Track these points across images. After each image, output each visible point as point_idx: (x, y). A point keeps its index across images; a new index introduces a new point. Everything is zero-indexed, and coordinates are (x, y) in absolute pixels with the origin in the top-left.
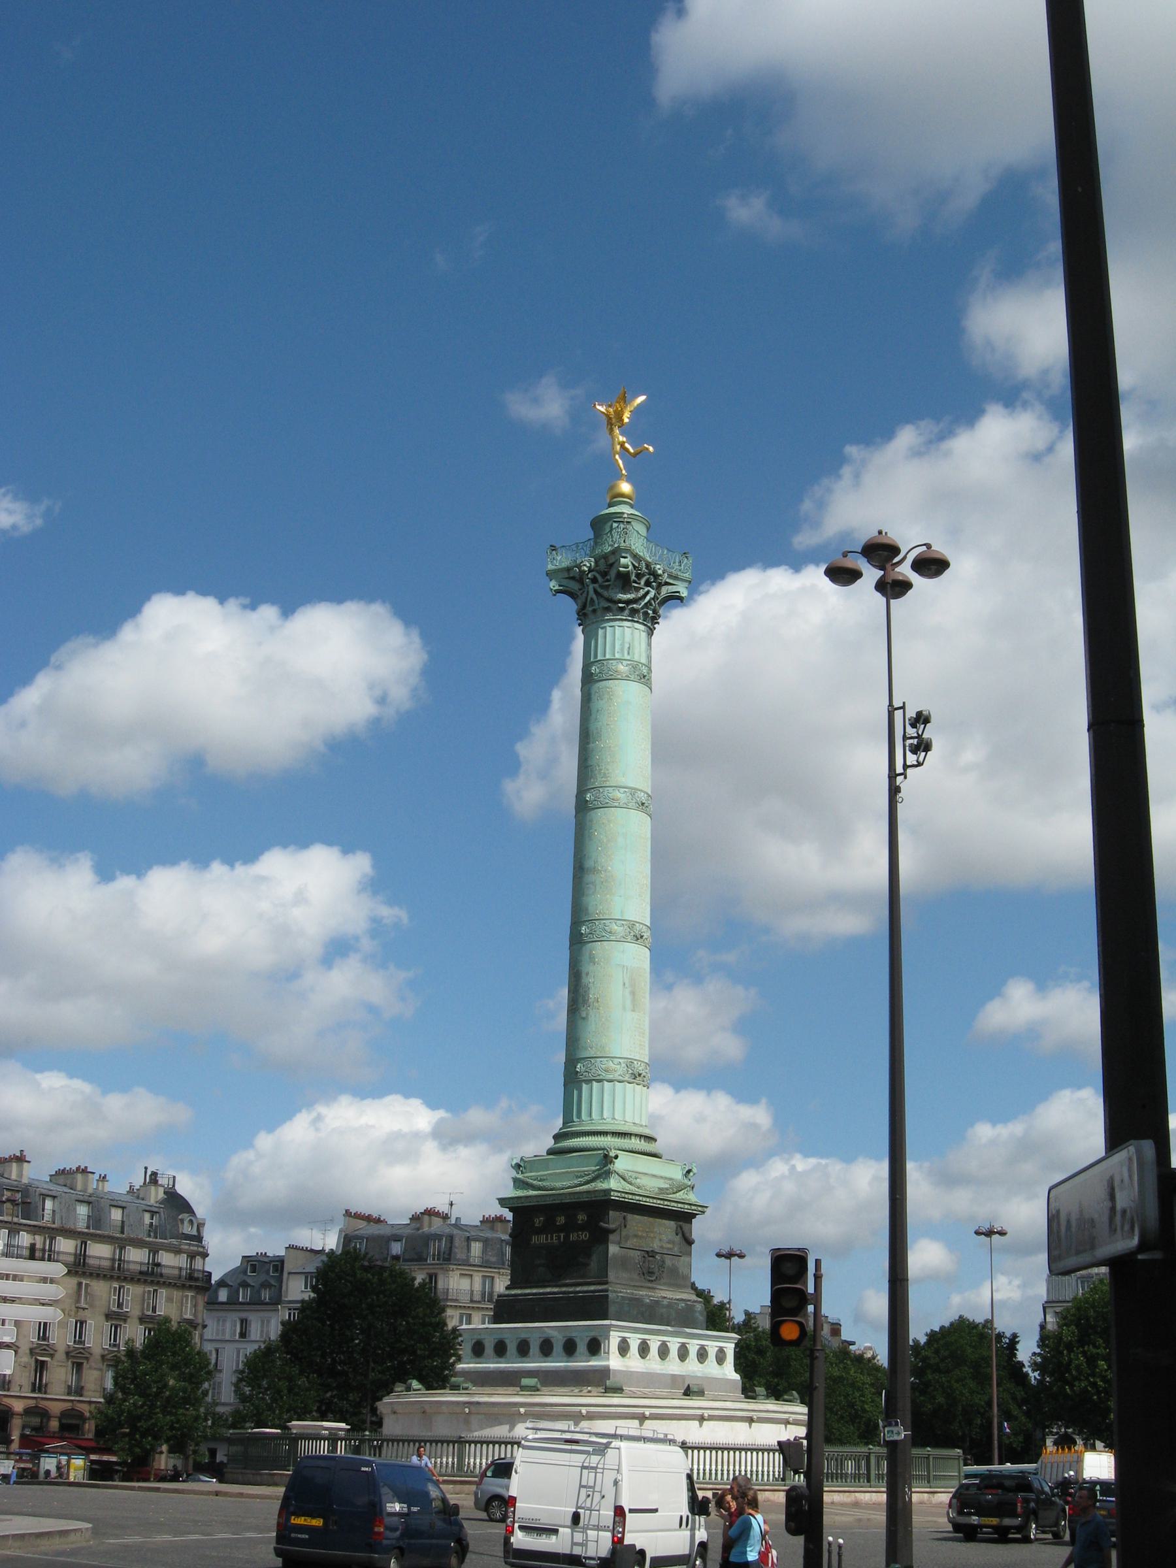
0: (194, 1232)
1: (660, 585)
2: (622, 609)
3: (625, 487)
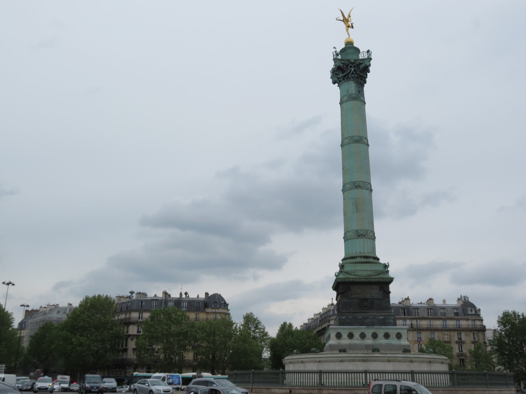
0: (473, 312)
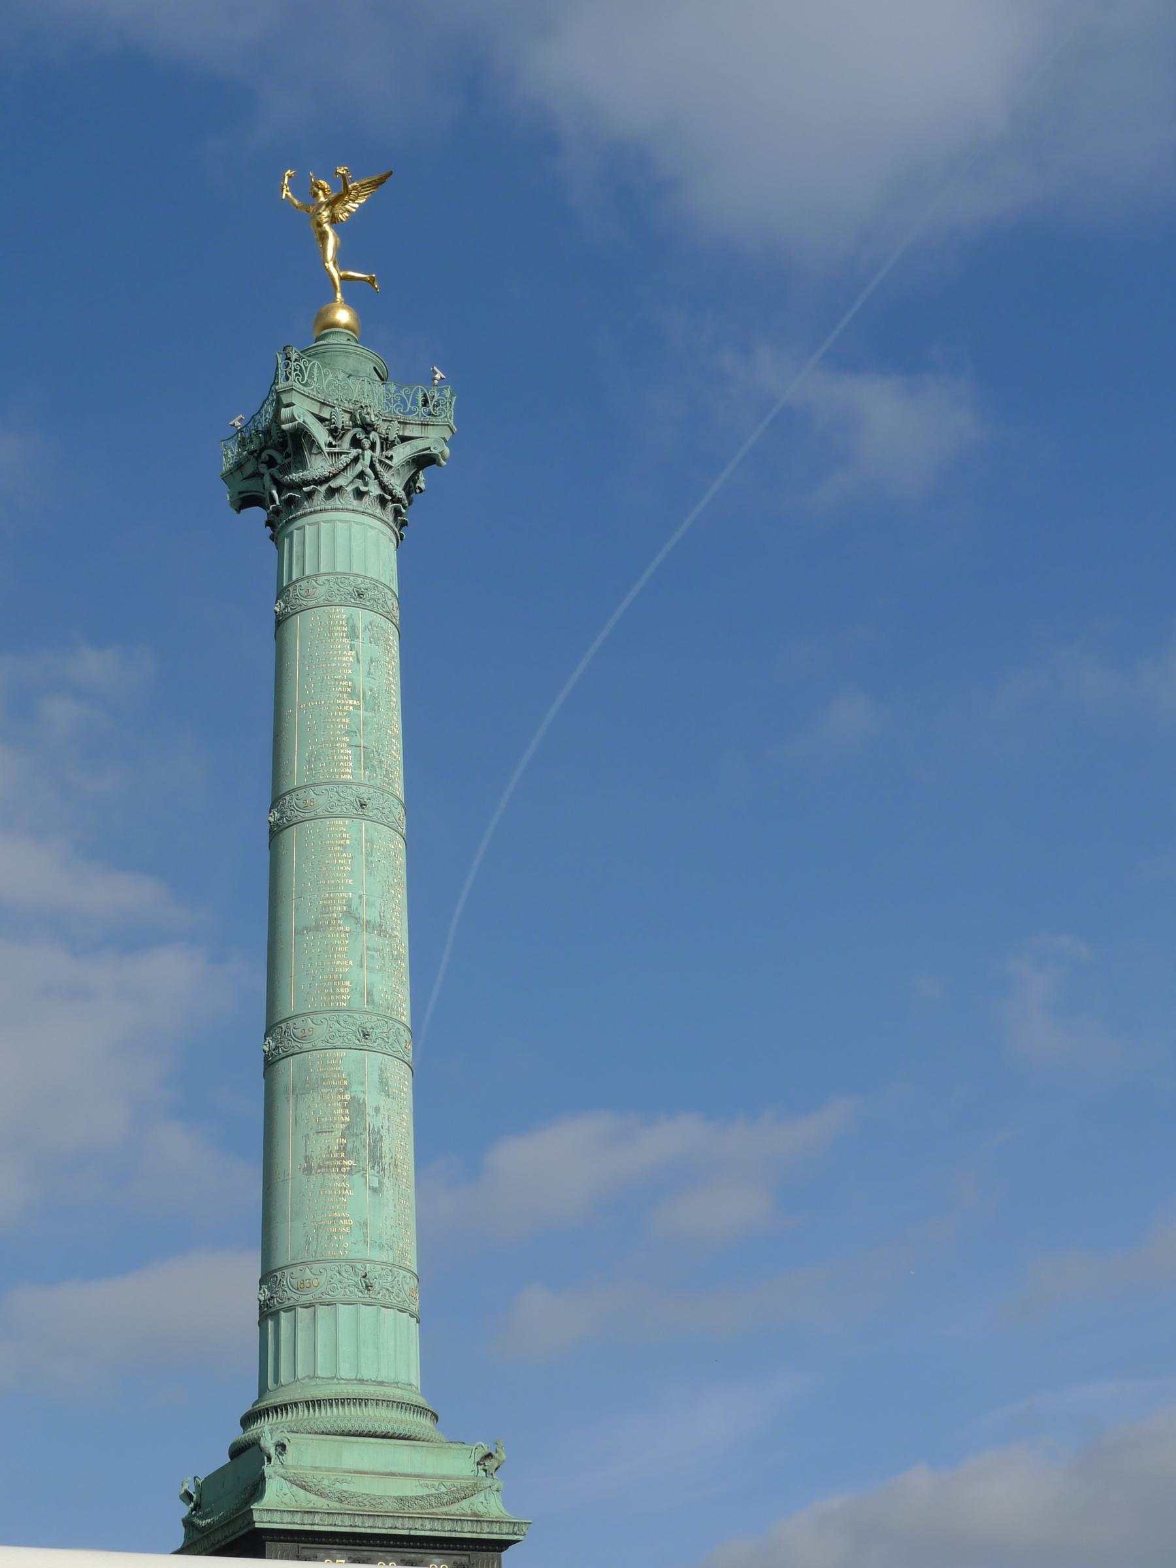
1: (387, 444)
2: (310, 495)
3: (343, 316)
